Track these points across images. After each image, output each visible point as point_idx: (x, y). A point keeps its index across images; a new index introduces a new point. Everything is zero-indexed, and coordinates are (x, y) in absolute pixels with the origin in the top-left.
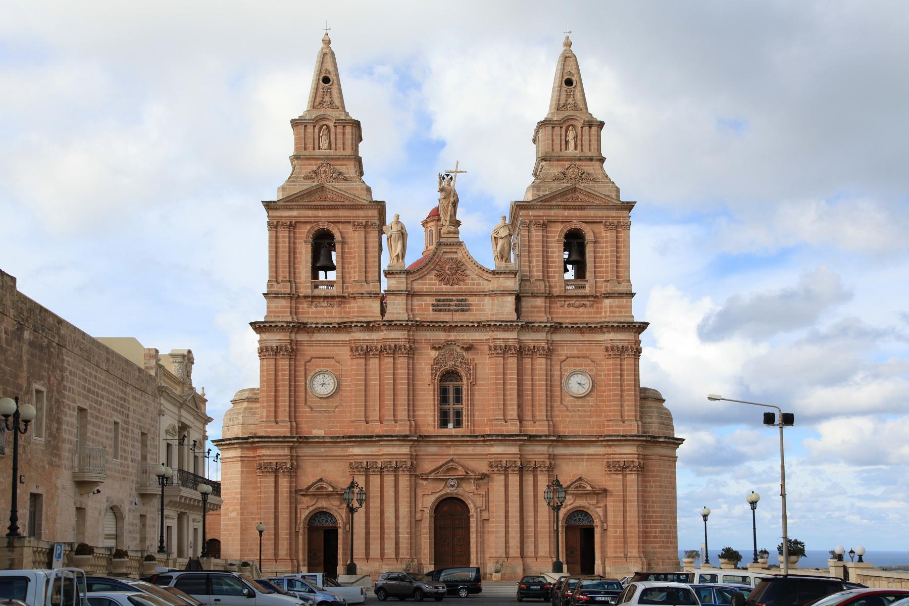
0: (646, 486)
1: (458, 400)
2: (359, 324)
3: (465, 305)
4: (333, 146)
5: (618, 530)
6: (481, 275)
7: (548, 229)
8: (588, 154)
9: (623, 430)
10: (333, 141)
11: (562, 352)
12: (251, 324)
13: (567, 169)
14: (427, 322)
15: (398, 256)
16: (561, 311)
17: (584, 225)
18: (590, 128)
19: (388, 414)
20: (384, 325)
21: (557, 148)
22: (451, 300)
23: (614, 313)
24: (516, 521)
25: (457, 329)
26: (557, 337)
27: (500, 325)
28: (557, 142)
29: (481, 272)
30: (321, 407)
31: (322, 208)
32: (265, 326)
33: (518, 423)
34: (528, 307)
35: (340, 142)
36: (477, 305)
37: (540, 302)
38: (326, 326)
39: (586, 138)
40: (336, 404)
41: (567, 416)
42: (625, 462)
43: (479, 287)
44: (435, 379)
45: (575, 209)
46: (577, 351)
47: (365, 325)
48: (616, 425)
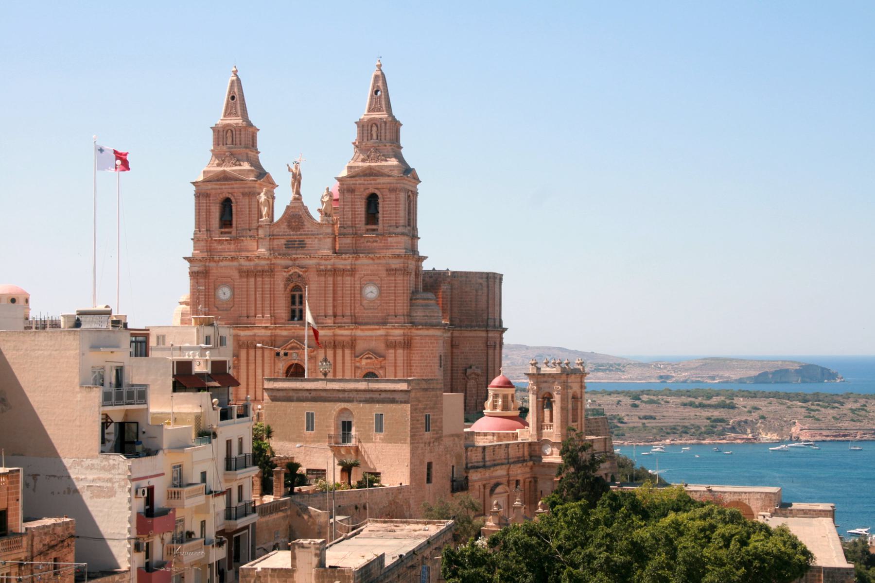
3: (303, 244)
4: (234, 142)
10: (234, 139)
22: (296, 241)
28: (365, 135)
30: (224, 307)
31: (225, 185)
36: (310, 244)
39: (383, 131)
40: (231, 306)
41: (364, 313)
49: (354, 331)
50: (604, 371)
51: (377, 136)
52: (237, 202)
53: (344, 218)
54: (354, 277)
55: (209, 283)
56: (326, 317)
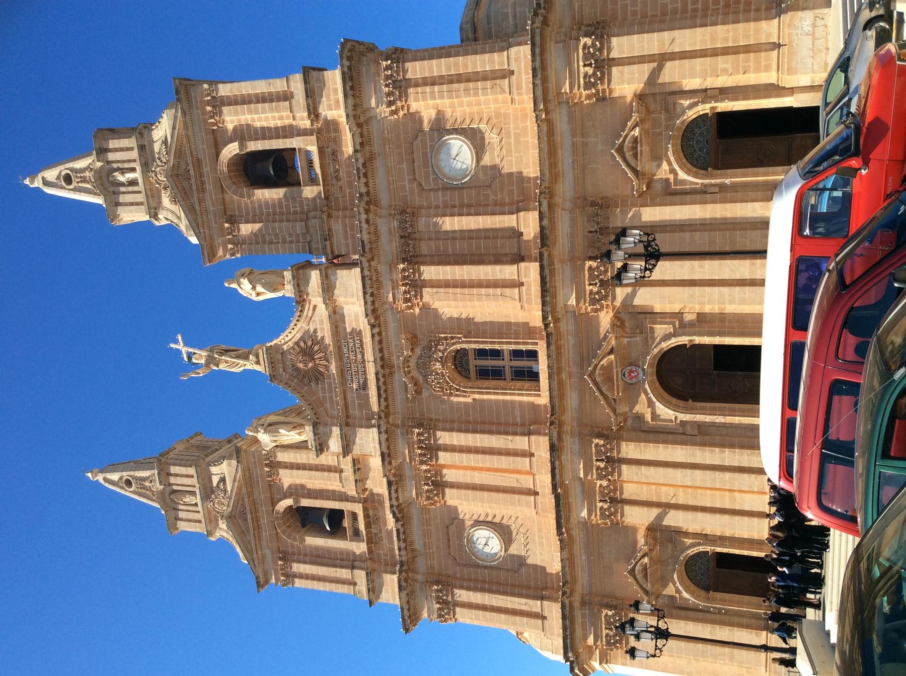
0: (634, 13)
1: (496, 354)
2: (394, 495)
5: (721, 66)
6: (308, 320)
7: (237, 213)
8: (135, 154)
9: (527, 73)
11: (407, 188)
12: (407, 630)
13: (160, 184)
14: (379, 402)
15: (299, 434)
16: (348, 191)
18: (108, 150)
19: (523, 463)
20: (390, 463)
21: (140, 198)
23: (338, 102)
24: (701, 267)
25: (386, 356)
26: (384, 198)
27: (372, 295)
29: (303, 318)
31: (256, 520)
32: (410, 617)
33: (523, 265)
34: (347, 244)
37: (337, 227)
38: (402, 537)
42: (585, 65)
43: (325, 322)
44: (465, 392)
45: (201, 175)
46: (402, 163)
47: (393, 488)
48: (519, 88)
49: (558, 200)
53: (291, 242)
54: (421, 207)
55: (463, 579)
56: (522, 284)
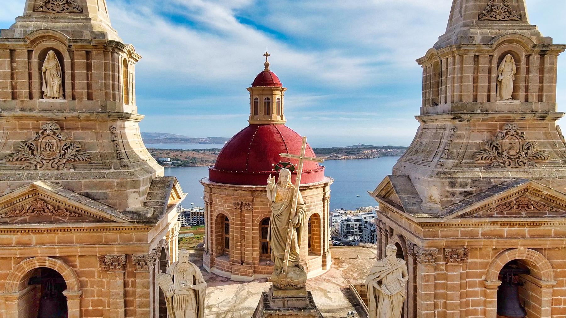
4: (68, 91)
7: (469, 260)
10: (68, 81)
17: (537, 254)
35: (80, 83)
50: (183, 141)
51: (516, 88)
52: (82, 285)
